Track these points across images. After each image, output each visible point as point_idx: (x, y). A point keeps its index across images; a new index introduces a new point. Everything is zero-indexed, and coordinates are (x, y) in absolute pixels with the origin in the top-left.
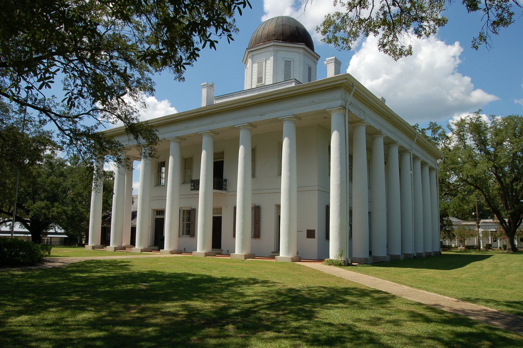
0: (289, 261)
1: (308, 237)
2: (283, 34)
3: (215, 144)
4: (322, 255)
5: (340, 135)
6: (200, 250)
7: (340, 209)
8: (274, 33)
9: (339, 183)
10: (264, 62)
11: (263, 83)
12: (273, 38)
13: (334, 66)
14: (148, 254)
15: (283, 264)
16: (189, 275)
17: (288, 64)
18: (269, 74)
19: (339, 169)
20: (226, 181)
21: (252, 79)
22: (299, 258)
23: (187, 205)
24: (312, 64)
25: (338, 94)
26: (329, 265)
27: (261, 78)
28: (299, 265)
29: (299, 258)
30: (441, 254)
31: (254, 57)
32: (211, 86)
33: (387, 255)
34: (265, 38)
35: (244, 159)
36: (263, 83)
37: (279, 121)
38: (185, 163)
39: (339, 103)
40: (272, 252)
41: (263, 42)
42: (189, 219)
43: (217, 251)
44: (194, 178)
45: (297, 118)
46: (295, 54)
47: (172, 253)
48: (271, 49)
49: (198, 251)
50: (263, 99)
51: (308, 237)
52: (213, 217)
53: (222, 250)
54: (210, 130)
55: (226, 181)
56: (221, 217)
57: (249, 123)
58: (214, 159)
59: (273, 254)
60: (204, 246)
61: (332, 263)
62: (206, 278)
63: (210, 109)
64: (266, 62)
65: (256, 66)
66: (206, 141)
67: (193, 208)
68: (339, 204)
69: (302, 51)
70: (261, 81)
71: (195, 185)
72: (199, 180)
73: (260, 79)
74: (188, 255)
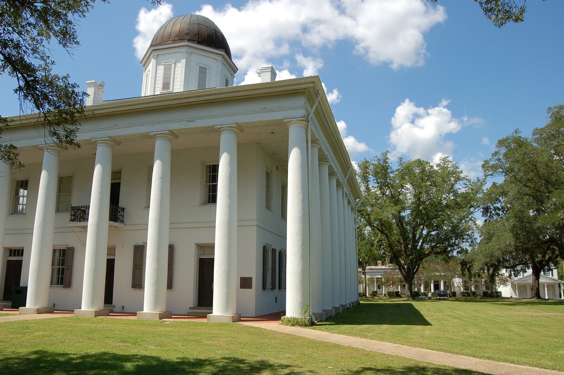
0: (229, 321)
1: (241, 287)
2: (198, 34)
3: (115, 157)
4: (278, 314)
5: (302, 154)
6: (85, 306)
7: (302, 249)
8: (187, 31)
9: (300, 215)
10: (173, 65)
11: (171, 90)
12: (187, 38)
13: (270, 75)
14: (7, 315)
15: (221, 325)
16: (128, 358)
17: (203, 71)
18: (179, 80)
19: (300, 197)
20: (123, 209)
21: (155, 84)
22: (238, 318)
23: (67, 241)
24: (229, 76)
25: (301, 101)
26: (293, 325)
27: (169, 84)
28: (245, 326)
29: (238, 318)
30: (359, 303)
31: (160, 57)
32: (100, 85)
33: (333, 308)
34: (176, 37)
35: (161, 178)
36: (171, 90)
37: (216, 131)
38: (60, 184)
39: (302, 112)
40: (190, 308)
41: (172, 40)
42: (62, 262)
43: (109, 307)
44: (75, 203)
45: (240, 128)
46: (210, 59)
47: (39, 312)
48: (183, 50)
49: (83, 308)
50: (195, 99)
51: (241, 287)
52: (108, 260)
53: (114, 306)
54: (110, 137)
55: (123, 209)
56: (114, 259)
57: (170, 130)
58: (112, 180)
59: (191, 311)
60: (93, 302)
61: (295, 323)
62: (155, 363)
63: (112, 108)
64: (175, 66)
65: (161, 69)
66: (102, 152)
67: (69, 246)
68: (300, 243)
69: (220, 58)
70: (168, 88)
71: (80, 214)
72: (88, 207)
73: (166, 85)
74: (65, 315)
